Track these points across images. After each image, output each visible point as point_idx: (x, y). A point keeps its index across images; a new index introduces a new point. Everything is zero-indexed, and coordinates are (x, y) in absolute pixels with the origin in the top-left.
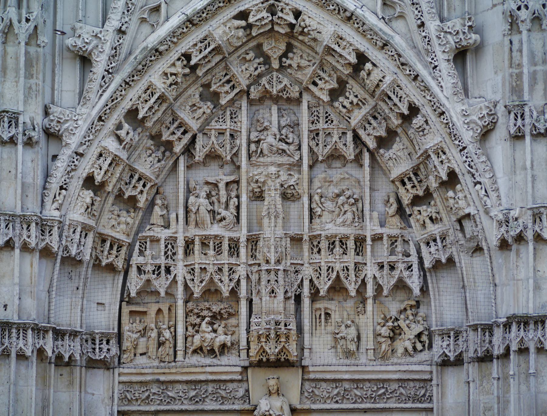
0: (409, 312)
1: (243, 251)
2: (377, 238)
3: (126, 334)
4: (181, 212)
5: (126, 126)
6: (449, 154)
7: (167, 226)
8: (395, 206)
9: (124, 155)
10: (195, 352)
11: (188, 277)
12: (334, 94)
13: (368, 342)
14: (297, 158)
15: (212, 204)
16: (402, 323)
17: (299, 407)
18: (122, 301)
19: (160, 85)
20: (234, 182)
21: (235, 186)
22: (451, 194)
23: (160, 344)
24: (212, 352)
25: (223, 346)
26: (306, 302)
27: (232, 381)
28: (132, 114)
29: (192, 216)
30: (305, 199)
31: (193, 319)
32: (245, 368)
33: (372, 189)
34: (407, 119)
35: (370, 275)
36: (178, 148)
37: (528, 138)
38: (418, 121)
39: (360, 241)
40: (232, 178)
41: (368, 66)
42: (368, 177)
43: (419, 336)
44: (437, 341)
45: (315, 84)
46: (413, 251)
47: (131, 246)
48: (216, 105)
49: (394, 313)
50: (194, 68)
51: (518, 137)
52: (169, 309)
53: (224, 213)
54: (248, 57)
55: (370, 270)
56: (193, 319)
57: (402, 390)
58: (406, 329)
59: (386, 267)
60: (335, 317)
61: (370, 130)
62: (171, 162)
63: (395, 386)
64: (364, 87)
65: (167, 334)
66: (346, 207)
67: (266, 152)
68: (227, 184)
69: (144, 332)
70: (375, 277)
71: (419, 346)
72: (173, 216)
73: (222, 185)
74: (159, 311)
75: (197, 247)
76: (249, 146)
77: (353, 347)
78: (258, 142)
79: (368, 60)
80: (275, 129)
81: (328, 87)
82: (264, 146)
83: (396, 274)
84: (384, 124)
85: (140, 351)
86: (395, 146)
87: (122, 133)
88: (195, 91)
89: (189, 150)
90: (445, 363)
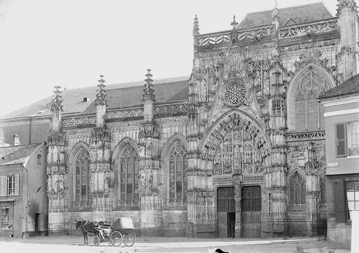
12: (247, 128)
19: (216, 129)
51: (273, 135)
55: (253, 158)
69: (217, 170)
75: (225, 156)
88: (223, 129)
89: (223, 139)
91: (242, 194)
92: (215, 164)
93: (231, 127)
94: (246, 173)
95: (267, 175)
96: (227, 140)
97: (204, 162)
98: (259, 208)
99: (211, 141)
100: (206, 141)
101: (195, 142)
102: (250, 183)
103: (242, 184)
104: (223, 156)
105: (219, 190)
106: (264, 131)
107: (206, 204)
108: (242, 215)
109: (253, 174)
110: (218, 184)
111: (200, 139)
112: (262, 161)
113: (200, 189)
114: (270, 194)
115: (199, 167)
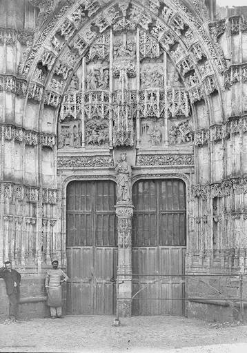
0: (183, 125)
1: (110, 99)
2: (169, 93)
3: (60, 136)
4: (84, 84)
5: (56, 39)
6: (202, 47)
7: (76, 89)
8: (178, 77)
9: (56, 53)
10: (90, 143)
11: (86, 110)
12: (151, 26)
13: (166, 137)
14: (134, 56)
15: (97, 79)
16: (180, 129)
17: (135, 167)
18: (58, 121)
19: (71, 19)
20: (107, 69)
21: (107, 71)
22: (203, 66)
23: (75, 140)
24: (97, 143)
25: (102, 141)
26: (138, 122)
27: (106, 156)
28: (58, 33)
29: (88, 84)
30: (138, 78)
31: (89, 129)
32: (111, 150)
33: (167, 72)
34: (183, 32)
35: (166, 108)
36: (81, 53)
37: (240, 33)
38: (188, 33)
39: (162, 94)
40: (106, 67)
41: (165, 8)
42: (165, 67)
43: (188, 134)
44: (196, 136)
45: (142, 22)
46: (185, 95)
47: (61, 98)
48: (98, 31)
49: (177, 125)
50: (86, 12)
52: (79, 126)
53: (103, 82)
54: (112, 10)
55: (167, 106)
56: (89, 129)
57: (181, 159)
58: (182, 132)
59: (174, 104)
60: (151, 127)
61: (166, 41)
62: (78, 61)
63: (176, 157)
64: (163, 21)
65: (77, 136)
66: (156, 78)
67: (120, 54)
68: (104, 70)
69: (68, 136)
70: (168, 110)
71: (188, 140)
72: (80, 84)
73: (101, 71)
74: (75, 126)
75: (90, 97)
76: (113, 52)
77: (159, 140)
78: (117, 50)
79: (165, 5)
80: (124, 45)
81: (148, 22)
82: (119, 52)
83: (178, 107)
84: (173, 38)
85: (66, 143)
86: (178, 48)
87: (54, 42)
88: (88, 26)
89: (86, 54)
90: (200, 146)
91: (135, 199)
92: (62, 117)
93: (109, 21)
94: (145, 144)
95: (203, 153)
96: (96, 58)
97: (33, 111)
98: (181, 236)
99: (56, 53)
100: (40, 51)
101: (9, 49)
102: (157, 171)
103: (137, 172)
104: (87, 100)
105: (72, 188)
106: (205, 26)
107: (39, 224)
108: (133, 253)
109: (165, 148)
110: (71, 173)
111: (23, 44)
112: (190, 115)
113: (21, 180)
114: (215, 199)
115: (18, 121)
